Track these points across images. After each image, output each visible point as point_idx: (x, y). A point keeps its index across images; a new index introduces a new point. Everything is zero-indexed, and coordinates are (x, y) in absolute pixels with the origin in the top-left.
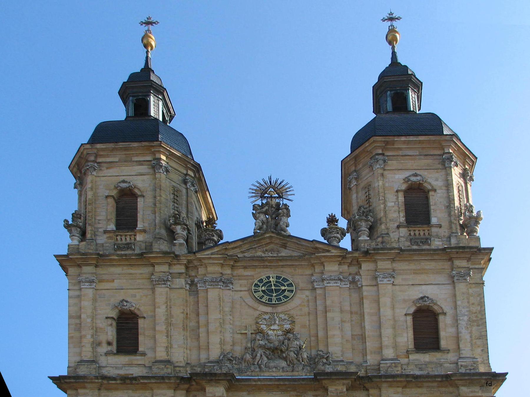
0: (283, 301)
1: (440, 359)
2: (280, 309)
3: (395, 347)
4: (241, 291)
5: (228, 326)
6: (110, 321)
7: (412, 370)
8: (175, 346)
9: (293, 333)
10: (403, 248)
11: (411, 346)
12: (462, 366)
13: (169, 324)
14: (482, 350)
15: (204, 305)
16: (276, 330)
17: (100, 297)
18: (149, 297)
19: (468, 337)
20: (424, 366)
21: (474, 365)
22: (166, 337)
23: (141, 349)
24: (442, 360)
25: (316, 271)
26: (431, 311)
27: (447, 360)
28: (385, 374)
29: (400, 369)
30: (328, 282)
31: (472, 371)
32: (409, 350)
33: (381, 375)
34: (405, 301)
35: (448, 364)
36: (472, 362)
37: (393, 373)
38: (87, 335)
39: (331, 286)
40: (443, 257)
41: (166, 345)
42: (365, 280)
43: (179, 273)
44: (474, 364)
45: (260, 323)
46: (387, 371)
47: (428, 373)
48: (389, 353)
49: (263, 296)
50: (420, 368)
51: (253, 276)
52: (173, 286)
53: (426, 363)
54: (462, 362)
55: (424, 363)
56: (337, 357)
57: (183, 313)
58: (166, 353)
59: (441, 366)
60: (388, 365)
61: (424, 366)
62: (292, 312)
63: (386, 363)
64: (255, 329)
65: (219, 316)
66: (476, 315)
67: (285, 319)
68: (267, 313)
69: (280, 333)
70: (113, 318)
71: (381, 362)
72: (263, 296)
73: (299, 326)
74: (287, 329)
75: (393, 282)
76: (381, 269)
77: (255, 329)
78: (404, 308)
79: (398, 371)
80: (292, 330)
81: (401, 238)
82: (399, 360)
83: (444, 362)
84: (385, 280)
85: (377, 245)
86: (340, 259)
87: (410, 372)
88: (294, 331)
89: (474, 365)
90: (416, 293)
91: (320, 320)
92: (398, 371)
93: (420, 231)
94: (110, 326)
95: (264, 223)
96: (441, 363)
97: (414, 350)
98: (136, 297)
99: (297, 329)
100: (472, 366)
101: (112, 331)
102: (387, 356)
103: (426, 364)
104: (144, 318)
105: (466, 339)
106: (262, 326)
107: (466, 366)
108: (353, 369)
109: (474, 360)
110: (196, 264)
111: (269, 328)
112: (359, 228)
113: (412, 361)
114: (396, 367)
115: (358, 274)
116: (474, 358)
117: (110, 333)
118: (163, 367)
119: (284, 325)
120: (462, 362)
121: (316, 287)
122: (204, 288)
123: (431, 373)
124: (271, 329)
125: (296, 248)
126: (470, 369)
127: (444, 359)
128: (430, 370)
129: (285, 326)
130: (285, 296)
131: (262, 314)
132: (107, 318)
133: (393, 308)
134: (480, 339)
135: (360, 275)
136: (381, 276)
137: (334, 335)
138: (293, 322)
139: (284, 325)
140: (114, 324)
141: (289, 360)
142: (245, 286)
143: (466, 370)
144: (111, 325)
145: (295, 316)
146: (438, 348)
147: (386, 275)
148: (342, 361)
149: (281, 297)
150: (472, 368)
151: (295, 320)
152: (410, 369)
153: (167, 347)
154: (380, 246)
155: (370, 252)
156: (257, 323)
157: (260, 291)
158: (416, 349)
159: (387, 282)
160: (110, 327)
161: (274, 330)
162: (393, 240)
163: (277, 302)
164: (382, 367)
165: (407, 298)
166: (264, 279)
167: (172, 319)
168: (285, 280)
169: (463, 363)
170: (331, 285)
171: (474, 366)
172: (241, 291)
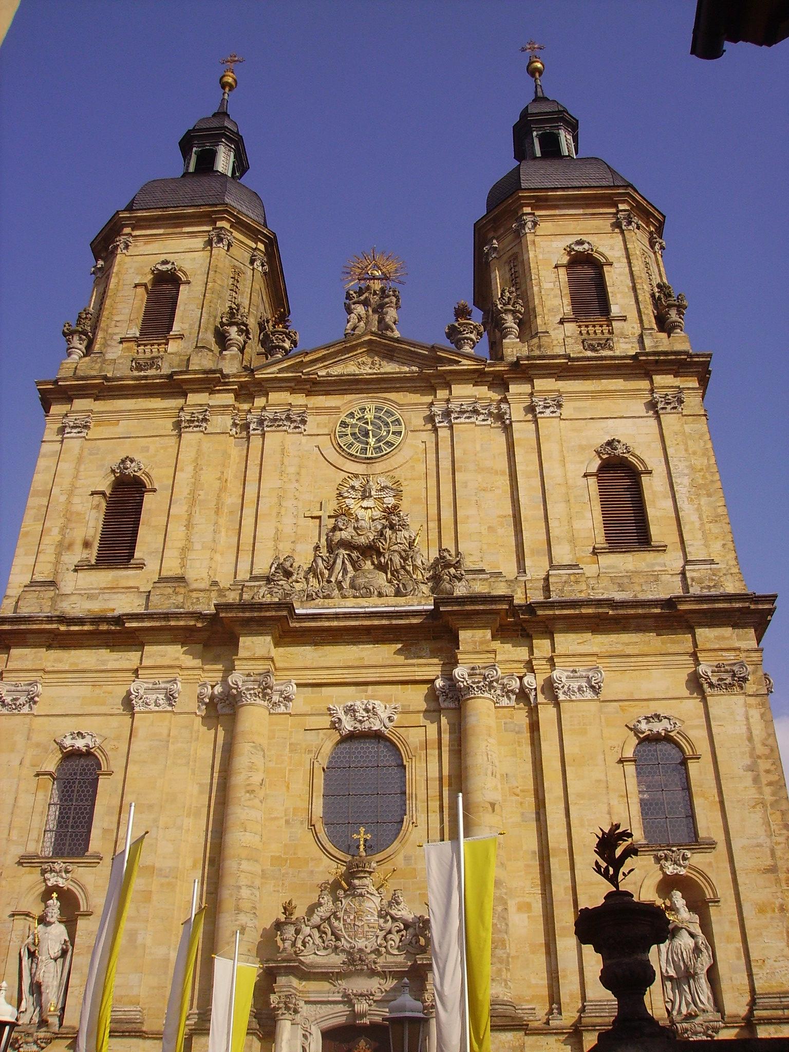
0: (385, 452)
1: (653, 565)
2: (379, 467)
3: (572, 540)
4: (318, 435)
5: (289, 503)
6: (97, 498)
7: (605, 588)
8: (197, 546)
9: (398, 515)
10: (572, 355)
11: (600, 539)
12: (693, 580)
13: (193, 501)
14: (724, 545)
15: (256, 462)
16: (371, 508)
17: (90, 454)
18: (170, 450)
19: (694, 518)
20: (626, 580)
21: (714, 578)
22: (184, 528)
23: (137, 555)
24: (657, 568)
25: (438, 397)
26: (628, 467)
27: (665, 566)
28: (560, 599)
29: (584, 587)
30: (456, 415)
31: (713, 592)
32: (596, 546)
33: (553, 602)
34: (582, 448)
35: (669, 576)
36: (709, 571)
37: (573, 597)
38: (53, 529)
39: (461, 423)
40: (636, 370)
41: (180, 544)
42: (516, 412)
43: (224, 406)
44: (714, 575)
45: (346, 495)
46: (562, 591)
47: (635, 596)
48: (562, 554)
49: (352, 444)
50: (620, 585)
51: (339, 408)
52: (210, 430)
53: (628, 574)
54: (693, 570)
55: (626, 574)
56: (474, 562)
57: (219, 479)
58: (180, 561)
59: (656, 581)
60: (564, 579)
61: (626, 580)
62: (397, 473)
63: (559, 575)
64: (336, 507)
65: (279, 484)
66: (702, 474)
67: (386, 487)
68: (356, 476)
69: (377, 514)
70: (103, 494)
71: (551, 572)
72: (352, 444)
73: (410, 499)
74: (390, 506)
75: (561, 414)
76: (540, 391)
77: (336, 507)
78: (582, 462)
79: (581, 592)
80: (398, 508)
81: (567, 339)
82: (582, 569)
83: (660, 571)
84: (548, 411)
85: (532, 350)
86: (476, 376)
87: (603, 594)
88: (400, 511)
89: (714, 578)
90: (599, 434)
91: (446, 488)
92: (581, 592)
93: (599, 331)
94: (94, 508)
95: (361, 318)
96: (656, 573)
97: (605, 545)
98: (148, 451)
99: (405, 507)
100: (711, 580)
101: (97, 519)
102: (559, 560)
103: (631, 575)
104: (154, 491)
105: (693, 523)
106: (347, 501)
107: (700, 581)
108: (501, 590)
109: (713, 566)
110: (251, 389)
111: (359, 505)
112: (504, 324)
113: (604, 571)
114: (577, 582)
115: (505, 400)
116: (712, 562)
117: (92, 524)
118: (170, 591)
119: (384, 498)
120: (693, 570)
121: (438, 425)
122: (259, 432)
123: (642, 597)
124: (362, 508)
125: (409, 358)
126: (709, 587)
127: (659, 564)
128: (638, 588)
129: (386, 500)
130: (388, 442)
131: (349, 477)
132: (93, 494)
133: (563, 462)
134: (716, 521)
135: (507, 402)
136: (540, 403)
137: (468, 517)
138: (398, 495)
139: (384, 498)
140: (104, 505)
141: (391, 571)
142: (326, 427)
143: (702, 588)
144: (98, 506)
145: (402, 480)
146: (647, 542)
147: (549, 401)
148: (482, 571)
149: (382, 445)
150: (712, 584)
151: (402, 488)
152: (603, 588)
153: (182, 549)
154: (537, 353)
155: (521, 362)
156: (340, 495)
157: (347, 435)
158: (609, 543)
159: (552, 415)
160: (94, 511)
161: (366, 508)
162: (555, 342)
163: (375, 455)
164: (553, 583)
165: (585, 443)
166: (356, 413)
167: (201, 492)
168: (389, 413)
169: (695, 574)
170: (462, 420)
171: (714, 580)
172: (318, 435)
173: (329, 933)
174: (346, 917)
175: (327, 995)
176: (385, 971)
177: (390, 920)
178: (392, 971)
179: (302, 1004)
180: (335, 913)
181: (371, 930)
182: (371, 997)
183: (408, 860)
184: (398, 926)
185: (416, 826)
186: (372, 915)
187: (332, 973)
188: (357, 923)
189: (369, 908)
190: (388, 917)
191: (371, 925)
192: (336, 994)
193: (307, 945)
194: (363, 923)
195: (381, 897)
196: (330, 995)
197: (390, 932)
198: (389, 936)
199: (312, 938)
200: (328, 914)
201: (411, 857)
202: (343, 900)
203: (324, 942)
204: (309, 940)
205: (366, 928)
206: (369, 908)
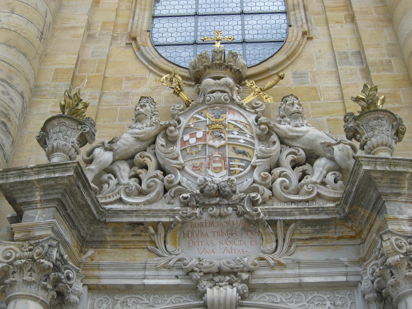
173: (152, 164)
174: (186, 138)
175: (141, 273)
176: (276, 221)
177: (278, 143)
178: (290, 222)
179: (78, 286)
180: (165, 128)
181: (241, 156)
182: (245, 276)
183: (299, 77)
184: (296, 155)
185: (308, 38)
186: (241, 132)
187: (155, 225)
188: (211, 142)
189: (236, 121)
190: (274, 138)
191: (241, 149)
192: (165, 272)
193: (106, 186)
194: (223, 142)
195: (256, 113)
196: (147, 273)
197: (278, 165)
198: (277, 171)
199: (116, 177)
200: (152, 130)
201: (306, 74)
202: (182, 119)
203: (140, 183)
204: (110, 178)
205: (229, 153)
206: (236, 121)
